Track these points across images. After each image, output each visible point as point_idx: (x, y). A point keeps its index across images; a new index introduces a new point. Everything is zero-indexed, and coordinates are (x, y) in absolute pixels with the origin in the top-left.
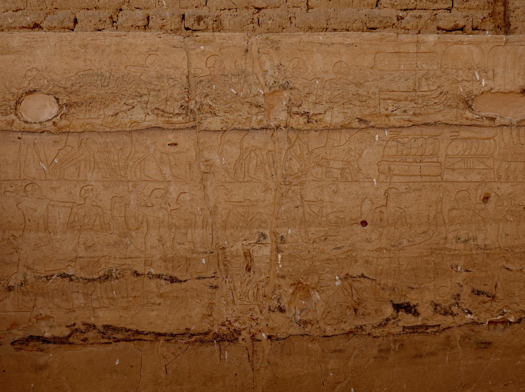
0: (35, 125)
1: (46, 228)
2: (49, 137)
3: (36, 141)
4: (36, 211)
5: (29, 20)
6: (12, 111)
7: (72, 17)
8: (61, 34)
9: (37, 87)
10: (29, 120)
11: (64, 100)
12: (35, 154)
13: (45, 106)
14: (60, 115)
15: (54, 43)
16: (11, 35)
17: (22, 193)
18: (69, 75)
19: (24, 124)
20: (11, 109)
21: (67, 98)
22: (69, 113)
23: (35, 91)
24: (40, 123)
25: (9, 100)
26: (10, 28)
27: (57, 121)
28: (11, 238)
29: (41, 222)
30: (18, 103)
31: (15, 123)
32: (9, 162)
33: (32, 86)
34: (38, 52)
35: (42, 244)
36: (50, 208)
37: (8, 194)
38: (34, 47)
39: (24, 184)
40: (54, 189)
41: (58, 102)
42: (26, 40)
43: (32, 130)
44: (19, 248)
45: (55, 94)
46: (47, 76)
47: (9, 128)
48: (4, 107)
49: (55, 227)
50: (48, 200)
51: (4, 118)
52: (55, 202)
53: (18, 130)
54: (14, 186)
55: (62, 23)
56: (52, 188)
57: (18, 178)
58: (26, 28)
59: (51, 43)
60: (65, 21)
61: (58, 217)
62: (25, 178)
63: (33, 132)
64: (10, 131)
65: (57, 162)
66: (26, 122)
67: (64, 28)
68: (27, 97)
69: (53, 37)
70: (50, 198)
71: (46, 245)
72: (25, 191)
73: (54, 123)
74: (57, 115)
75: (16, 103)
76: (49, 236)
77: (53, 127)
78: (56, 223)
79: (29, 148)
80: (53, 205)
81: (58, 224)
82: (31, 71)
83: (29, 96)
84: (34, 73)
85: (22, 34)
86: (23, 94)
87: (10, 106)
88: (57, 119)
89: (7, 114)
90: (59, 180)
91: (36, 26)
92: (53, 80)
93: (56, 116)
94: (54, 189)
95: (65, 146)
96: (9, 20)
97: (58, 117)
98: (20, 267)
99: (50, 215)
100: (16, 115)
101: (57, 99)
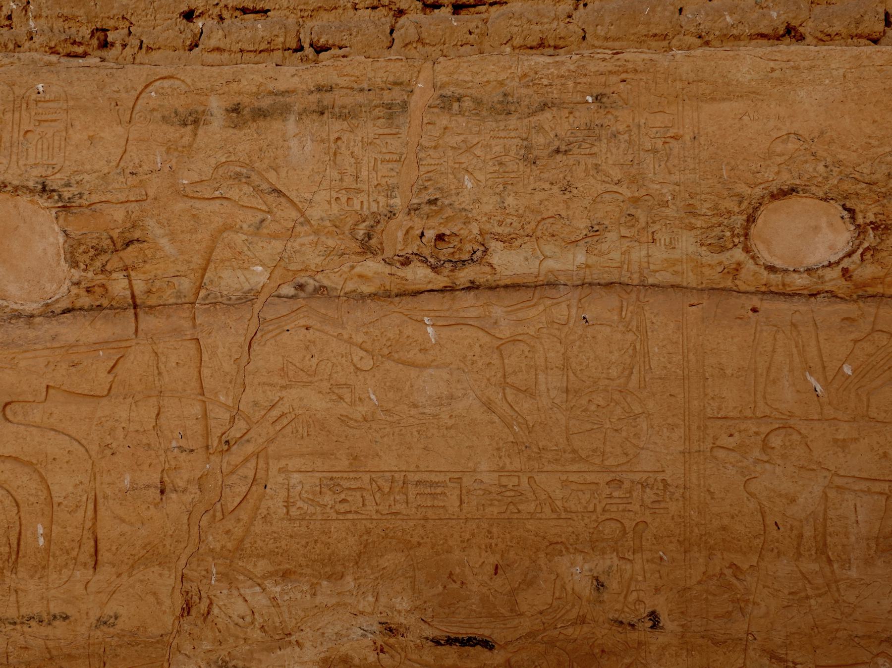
0: (796, 276)
1: (822, 550)
2: (829, 308)
3: (797, 317)
4: (793, 501)
5: (777, 17)
6: (736, 240)
7: (881, 10)
8: (855, 50)
9: (798, 182)
10: (778, 264)
11: (869, 213)
12: (795, 350)
13: (817, 229)
14: (860, 251)
15: (841, 71)
16: (731, 53)
17: (757, 453)
18: (880, 151)
19: (765, 273)
20: (733, 236)
21: (877, 209)
22: (883, 246)
23: (793, 190)
24: (809, 270)
25: (729, 212)
26: (730, 38)
27: (852, 267)
28: (728, 572)
29: (808, 532)
30: (751, 219)
31: (744, 271)
32: (729, 372)
33: (787, 179)
34: (802, 93)
35: (810, 592)
36: (832, 494)
37: (721, 454)
38: (790, 83)
39: (764, 429)
40: (843, 444)
41: (853, 218)
42: (772, 64)
43: (788, 290)
44: (747, 601)
45: (846, 198)
46: (825, 154)
47: (729, 284)
48: (717, 231)
49: (843, 546)
50: (826, 473)
51: (717, 258)
52: (845, 480)
53: (753, 289)
54: (736, 434)
55: (858, 23)
56: (836, 441)
57: (748, 413)
58: (763, 36)
59: (835, 73)
60: (866, 18)
61: (853, 519)
62: (768, 412)
63: (791, 295)
64: (731, 290)
65: (850, 373)
66: (771, 269)
67: (859, 36)
68: (771, 206)
69: (839, 57)
70: (832, 468)
71: (820, 596)
72: (765, 446)
73: (845, 271)
74: (854, 252)
75: (748, 221)
76: (827, 570)
77: (842, 282)
78: (847, 535)
79: (780, 336)
80: (838, 487)
81: (853, 539)
82: (785, 142)
83: (777, 203)
84: (791, 146)
85: (760, 51)
86: (763, 197)
87: (732, 230)
88: (853, 262)
89: (723, 249)
90: (854, 420)
91: (791, 33)
92: (840, 163)
93: (849, 255)
94: (843, 444)
95: (873, 330)
96: (728, 19)
97: (856, 257)
98: (751, 653)
99: (831, 514)
100: (747, 250)
101: (851, 211)
